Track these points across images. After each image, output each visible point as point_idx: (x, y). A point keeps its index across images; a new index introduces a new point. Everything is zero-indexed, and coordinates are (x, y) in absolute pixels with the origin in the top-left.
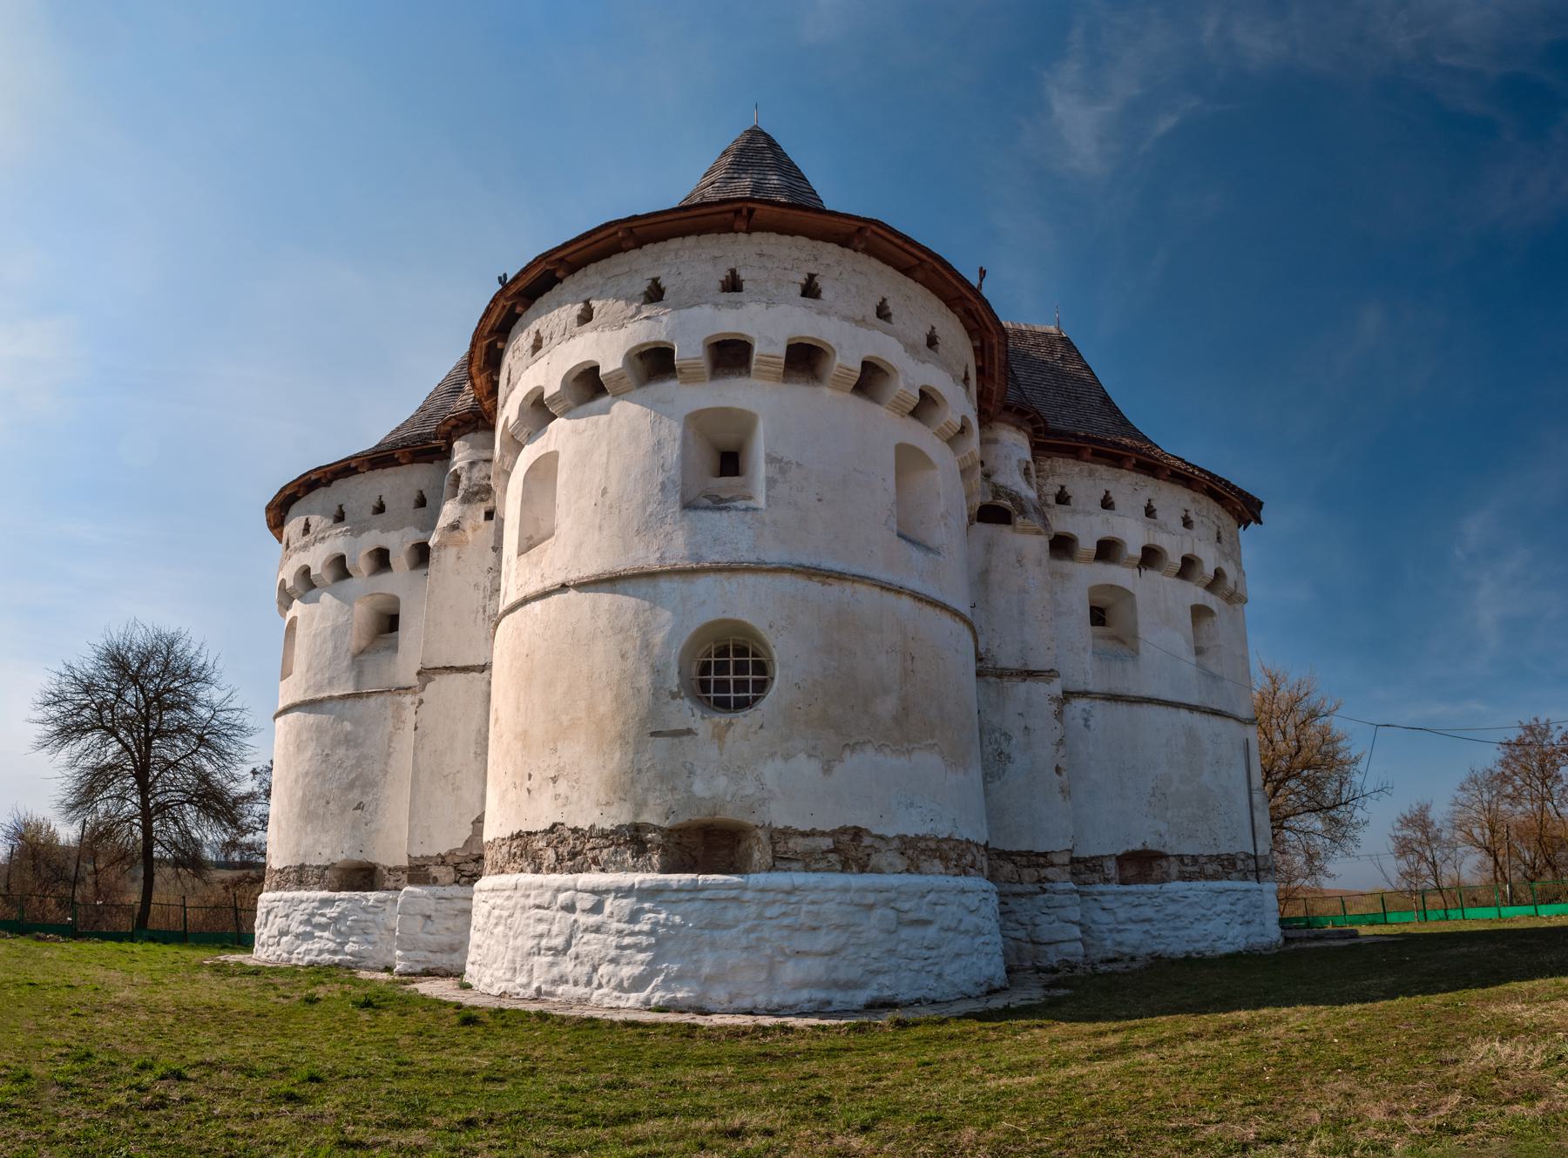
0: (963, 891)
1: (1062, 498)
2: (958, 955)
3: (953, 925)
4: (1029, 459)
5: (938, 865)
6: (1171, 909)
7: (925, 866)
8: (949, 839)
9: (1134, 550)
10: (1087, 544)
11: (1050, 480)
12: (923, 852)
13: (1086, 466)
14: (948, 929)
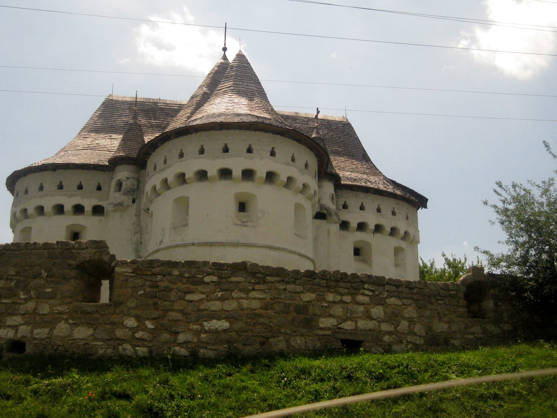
1: (345, 207)
4: (333, 192)
9: (372, 227)
10: (354, 225)
11: (340, 199)
13: (355, 193)
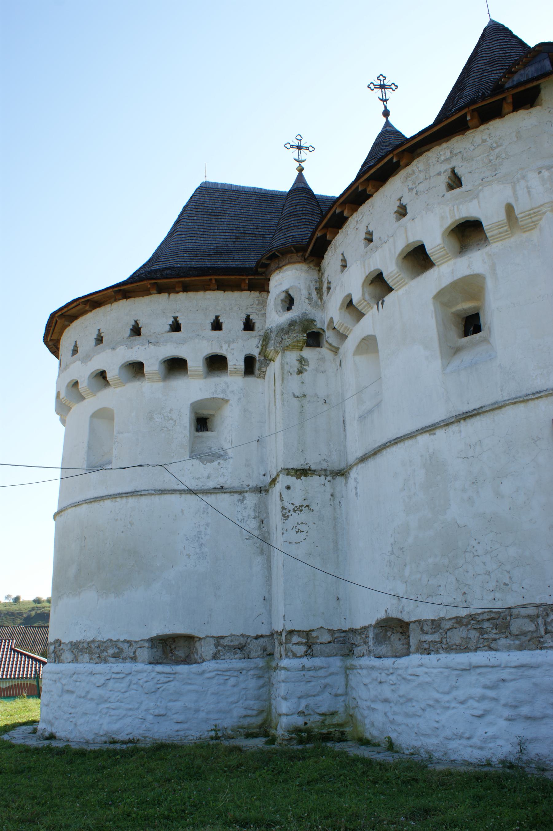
0: (92, 674)
2: (85, 714)
3: (83, 694)
5: (86, 657)
6: (404, 689)
7: (80, 658)
8: (93, 641)
12: (81, 651)
14: (80, 697)
